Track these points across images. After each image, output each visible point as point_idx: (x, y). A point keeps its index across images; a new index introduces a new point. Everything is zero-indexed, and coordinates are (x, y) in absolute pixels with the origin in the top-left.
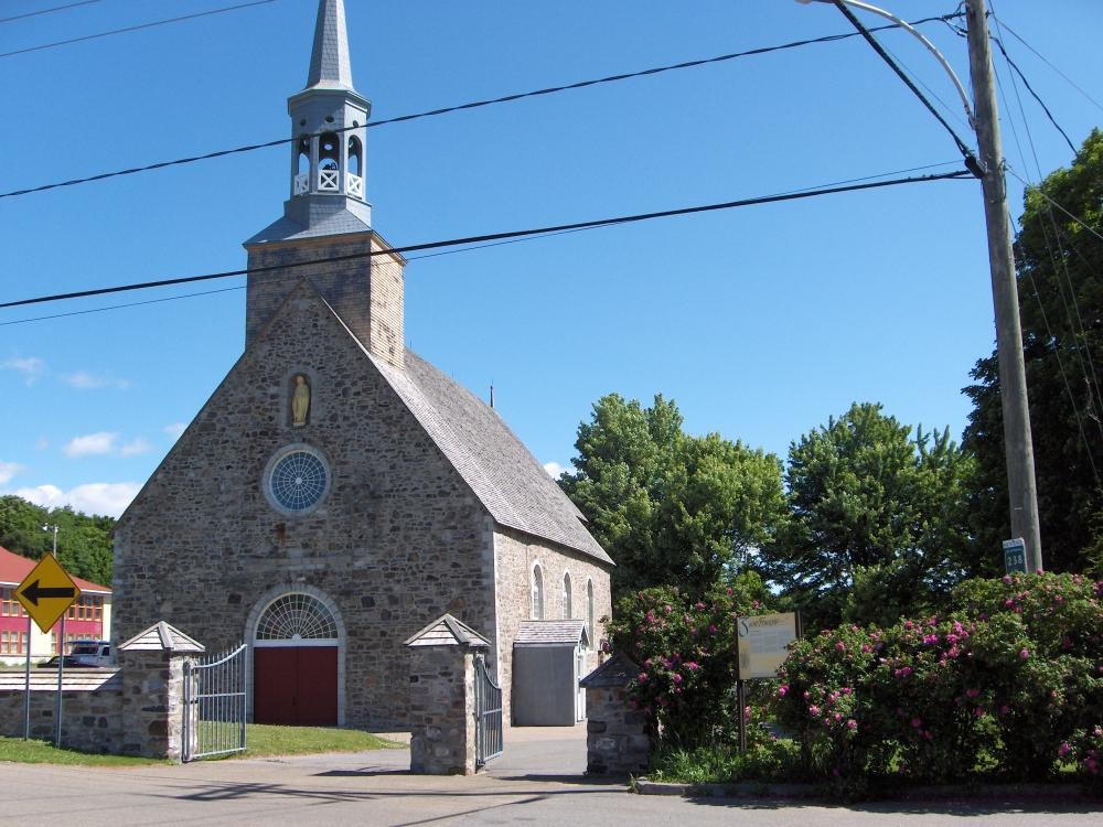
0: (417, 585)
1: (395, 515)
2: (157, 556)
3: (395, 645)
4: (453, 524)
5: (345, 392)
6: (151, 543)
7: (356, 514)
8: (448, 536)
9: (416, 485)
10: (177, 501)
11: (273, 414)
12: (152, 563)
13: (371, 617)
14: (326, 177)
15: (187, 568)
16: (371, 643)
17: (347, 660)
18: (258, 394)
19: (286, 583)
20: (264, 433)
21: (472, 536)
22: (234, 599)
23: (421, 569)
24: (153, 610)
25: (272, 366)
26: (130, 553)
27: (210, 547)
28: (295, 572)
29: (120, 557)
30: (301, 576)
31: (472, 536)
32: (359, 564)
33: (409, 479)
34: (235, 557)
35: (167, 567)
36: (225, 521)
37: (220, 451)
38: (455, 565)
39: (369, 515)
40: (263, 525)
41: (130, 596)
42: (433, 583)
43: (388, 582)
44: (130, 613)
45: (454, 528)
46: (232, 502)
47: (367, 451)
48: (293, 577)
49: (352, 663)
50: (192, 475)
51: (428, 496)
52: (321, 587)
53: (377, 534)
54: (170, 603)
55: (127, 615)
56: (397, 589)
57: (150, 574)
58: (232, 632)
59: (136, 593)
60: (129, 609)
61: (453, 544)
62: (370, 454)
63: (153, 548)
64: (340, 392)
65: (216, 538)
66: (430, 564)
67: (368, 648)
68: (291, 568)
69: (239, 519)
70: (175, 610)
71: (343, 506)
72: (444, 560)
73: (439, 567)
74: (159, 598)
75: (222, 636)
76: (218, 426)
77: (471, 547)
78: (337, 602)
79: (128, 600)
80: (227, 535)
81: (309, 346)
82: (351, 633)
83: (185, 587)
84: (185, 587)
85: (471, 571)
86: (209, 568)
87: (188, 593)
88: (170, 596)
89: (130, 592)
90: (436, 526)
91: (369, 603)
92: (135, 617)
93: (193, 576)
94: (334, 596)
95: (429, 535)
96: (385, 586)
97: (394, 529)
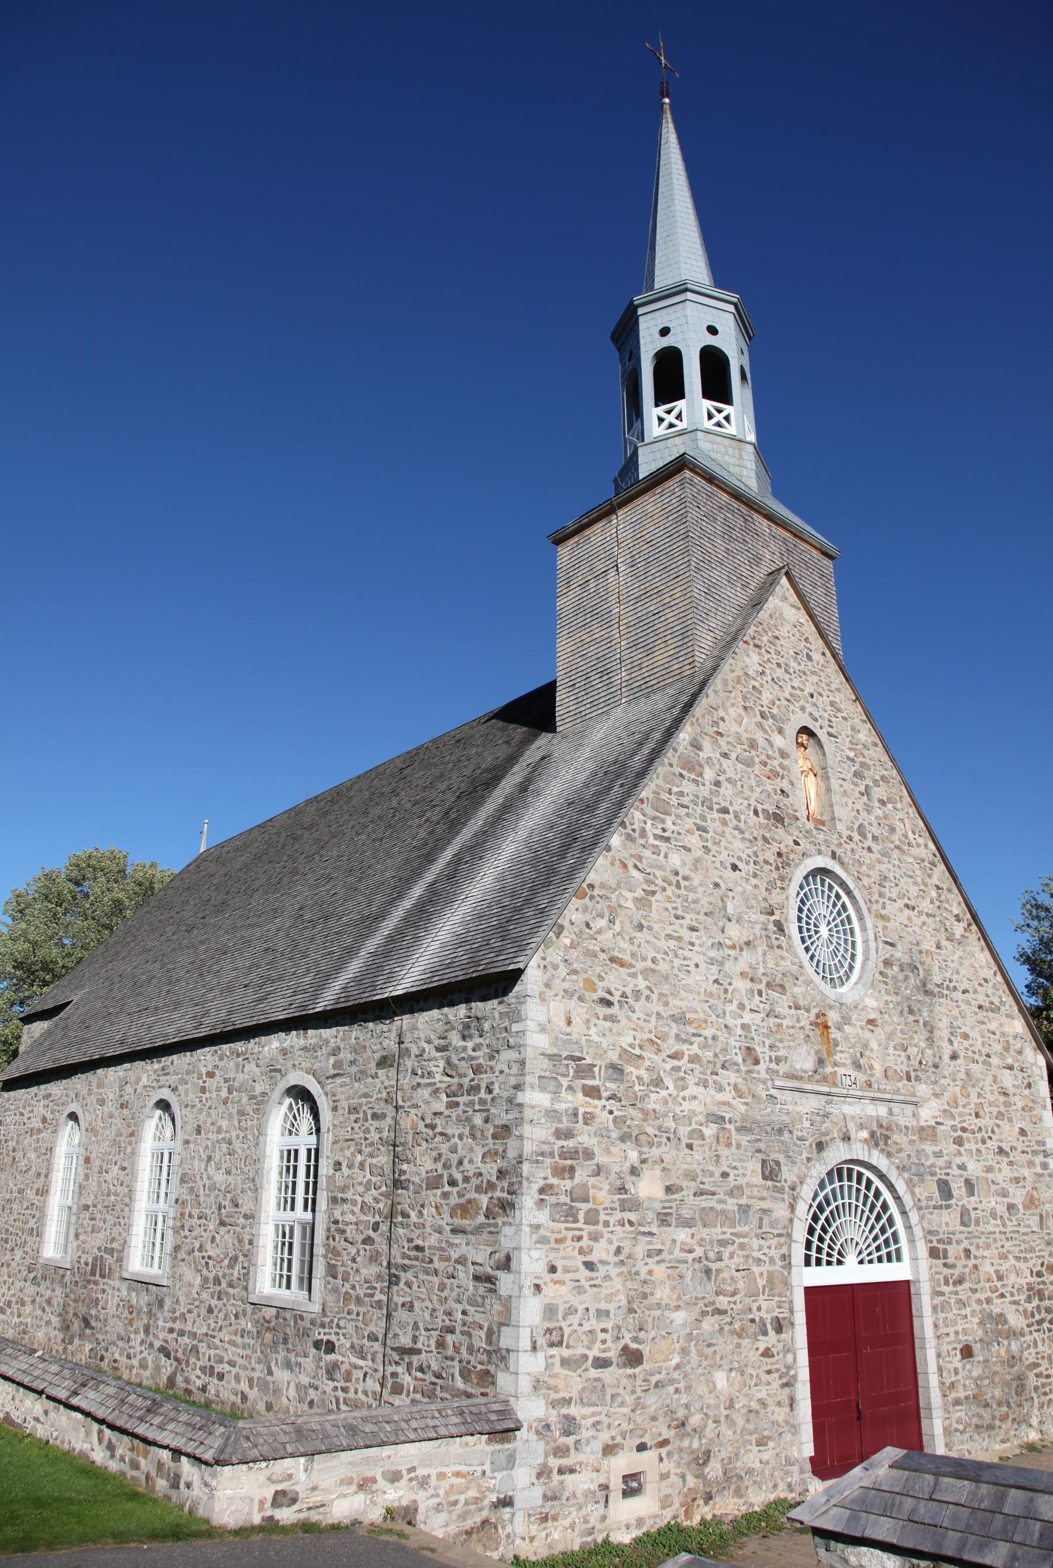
0: (990, 1163)
1: (953, 1029)
2: (626, 1041)
3: (982, 1277)
4: (1010, 1061)
5: (867, 792)
6: (609, 1004)
7: (911, 1018)
8: (1008, 1080)
9: (965, 985)
10: (654, 914)
11: (785, 785)
12: (613, 1056)
13: (947, 1220)
14: (724, 422)
15: (681, 1084)
16: (956, 1272)
17: (934, 1308)
18: (759, 737)
19: (844, 1139)
20: (778, 818)
21: (1029, 1086)
22: (770, 1172)
23: (990, 1134)
24: (622, 1190)
25: (770, 697)
26: (562, 1022)
27: (722, 1036)
28: (853, 1117)
29: (543, 1029)
30: (861, 1127)
31: (1029, 1086)
32: (928, 1114)
33: (958, 973)
34: (762, 1067)
35: (642, 1072)
36: (742, 985)
37: (720, 828)
38: (1023, 1132)
39: (925, 1024)
40: (797, 1008)
41: (570, 1143)
42: (1006, 1160)
43: (959, 1153)
44: (570, 1193)
45: (1011, 1068)
46: (748, 943)
47: (907, 906)
48: (852, 1127)
49: (942, 1315)
50: (675, 860)
51: (980, 1007)
52: (889, 1155)
53: (937, 1060)
54: (658, 1172)
55: (564, 1199)
56: (974, 1168)
57: (612, 1086)
58: (773, 1252)
59: (585, 1138)
60: (568, 1184)
61: (1014, 1094)
62: (910, 912)
63: (612, 1018)
64: (862, 789)
65: (731, 1022)
66: (998, 1126)
67: (954, 1284)
68: (847, 1110)
69: (762, 987)
70: (669, 1189)
71: (894, 998)
72: (1010, 1120)
73: (1008, 1133)
74: (633, 1156)
75: (759, 1261)
76: (709, 775)
77: (1031, 1105)
78: (910, 1185)
79: (563, 1155)
80: (747, 1018)
81: (809, 689)
82: (934, 1253)
83: (683, 1131)
84: (683, 1131)
85: (1038, 1142)
86: (721, 1089)
87: (690, 1146)
88: (655, 1153)
89: (569, 1134)
90: (994, 1060)
91: (945, 1190)
92: (584, 1207)
93: (694, 1105)
94: (906, 1175)
95: (990, 1079)
96: (958, 1160)
97: (954, 1057)
